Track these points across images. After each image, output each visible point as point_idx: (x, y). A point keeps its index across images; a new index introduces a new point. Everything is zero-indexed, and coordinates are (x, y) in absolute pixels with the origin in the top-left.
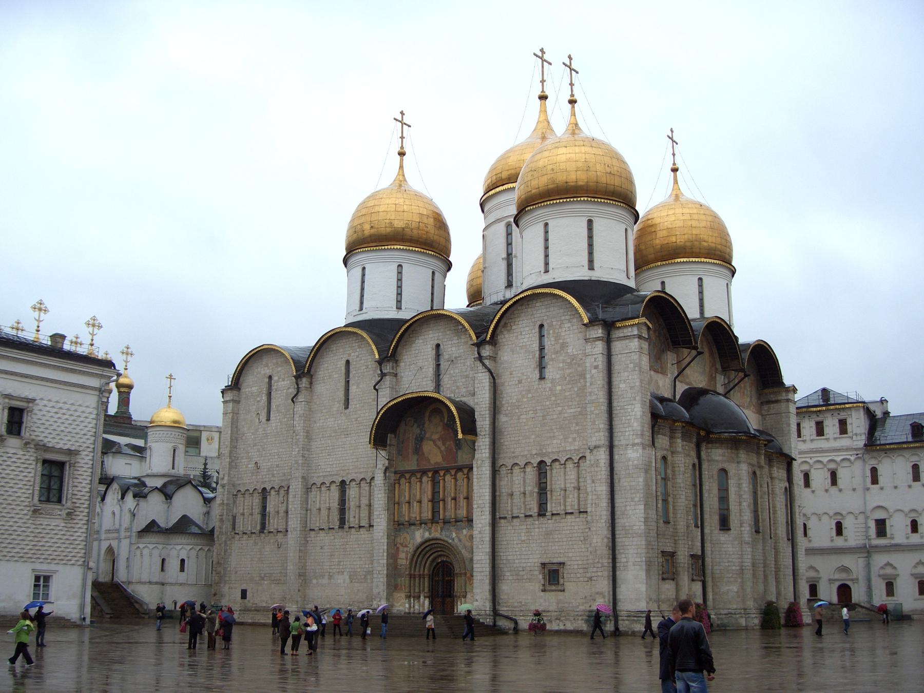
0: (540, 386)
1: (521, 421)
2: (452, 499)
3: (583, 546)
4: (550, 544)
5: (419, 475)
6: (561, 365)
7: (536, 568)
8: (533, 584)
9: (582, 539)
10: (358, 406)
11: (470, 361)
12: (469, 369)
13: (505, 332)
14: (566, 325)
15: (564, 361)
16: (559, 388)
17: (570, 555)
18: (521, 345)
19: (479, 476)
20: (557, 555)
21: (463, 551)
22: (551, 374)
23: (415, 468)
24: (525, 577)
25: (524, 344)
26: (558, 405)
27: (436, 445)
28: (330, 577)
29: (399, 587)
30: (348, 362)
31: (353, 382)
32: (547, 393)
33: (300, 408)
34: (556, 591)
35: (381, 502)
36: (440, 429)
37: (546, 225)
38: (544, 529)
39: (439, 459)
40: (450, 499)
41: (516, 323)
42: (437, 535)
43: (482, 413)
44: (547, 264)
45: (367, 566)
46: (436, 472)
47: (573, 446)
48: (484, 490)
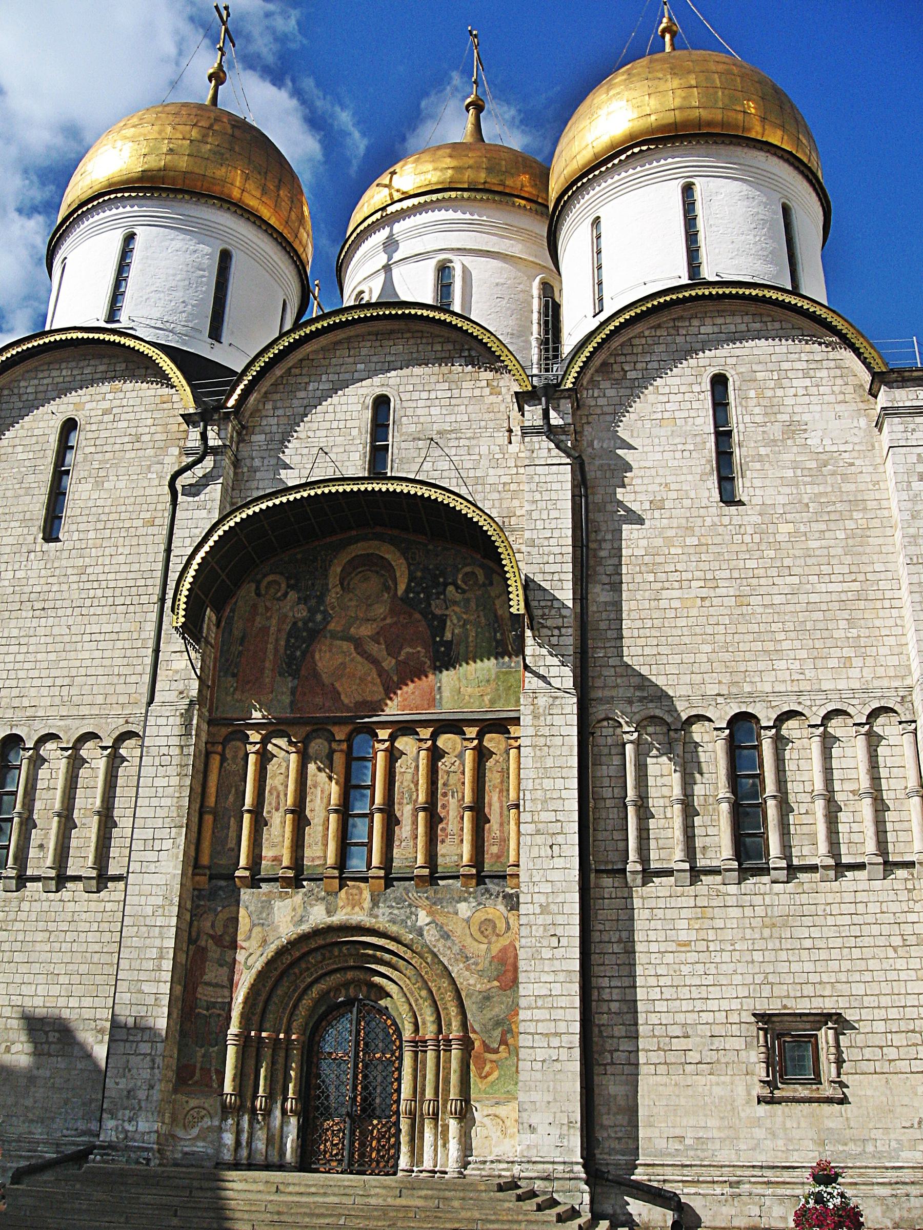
0: (726, 520)
1: (663, 604)
3: (901, 964)
4: (783, 955)
6: (790, 473)
7: (735, 1029)
8: (727, 1079)
9: (897, 941)
10: (92, 535)
12: (484, 462)
13: (605, 384)
14: (795, 383)
15: (795, 466)
16: (784, 528)
17: (859, 989)
18: (659, 416)
19: (542, 741)
20: (808, 990)
22: (758, 492)
24: (693, 1057)
25: (666, 415)
29: (197, 1076)
30: (70, 426)
31: (82, 474)
32: (747, 539)
34: (810, 1100)
35: (166, 802)
36: (380, 610)
38: (760, 911)
41: (639, 366)
42: (359, 917)
43: (547, 568)
45: (73, 1002)
48: (560, 783)
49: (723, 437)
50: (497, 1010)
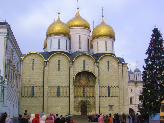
2: (88, 92)
5: (80, 87)
11: (92, 65)
21: (91, 103)
23: (79, 85)
26: (112, 77)
27: (84, 81)
28: (55, 107)
33: (46, 69)
36: (85, 78)
37: (106, 41)
39: (85, 84)
40: (87, 92)
42: (85, 99)
44: (106, 49)
46: (84, 86)
47: (115, 84)
49: (108, 65)
50: (94, 105)
